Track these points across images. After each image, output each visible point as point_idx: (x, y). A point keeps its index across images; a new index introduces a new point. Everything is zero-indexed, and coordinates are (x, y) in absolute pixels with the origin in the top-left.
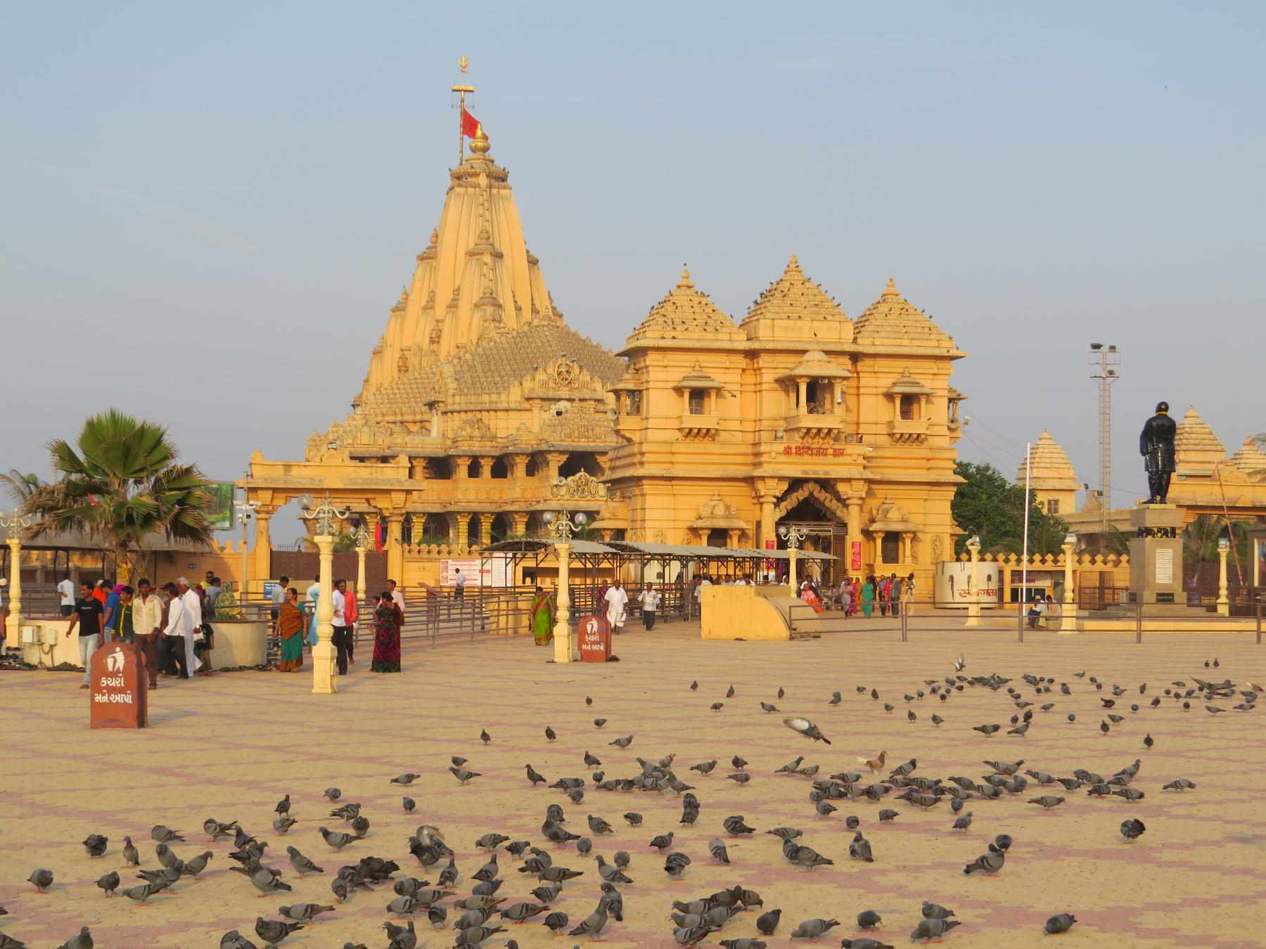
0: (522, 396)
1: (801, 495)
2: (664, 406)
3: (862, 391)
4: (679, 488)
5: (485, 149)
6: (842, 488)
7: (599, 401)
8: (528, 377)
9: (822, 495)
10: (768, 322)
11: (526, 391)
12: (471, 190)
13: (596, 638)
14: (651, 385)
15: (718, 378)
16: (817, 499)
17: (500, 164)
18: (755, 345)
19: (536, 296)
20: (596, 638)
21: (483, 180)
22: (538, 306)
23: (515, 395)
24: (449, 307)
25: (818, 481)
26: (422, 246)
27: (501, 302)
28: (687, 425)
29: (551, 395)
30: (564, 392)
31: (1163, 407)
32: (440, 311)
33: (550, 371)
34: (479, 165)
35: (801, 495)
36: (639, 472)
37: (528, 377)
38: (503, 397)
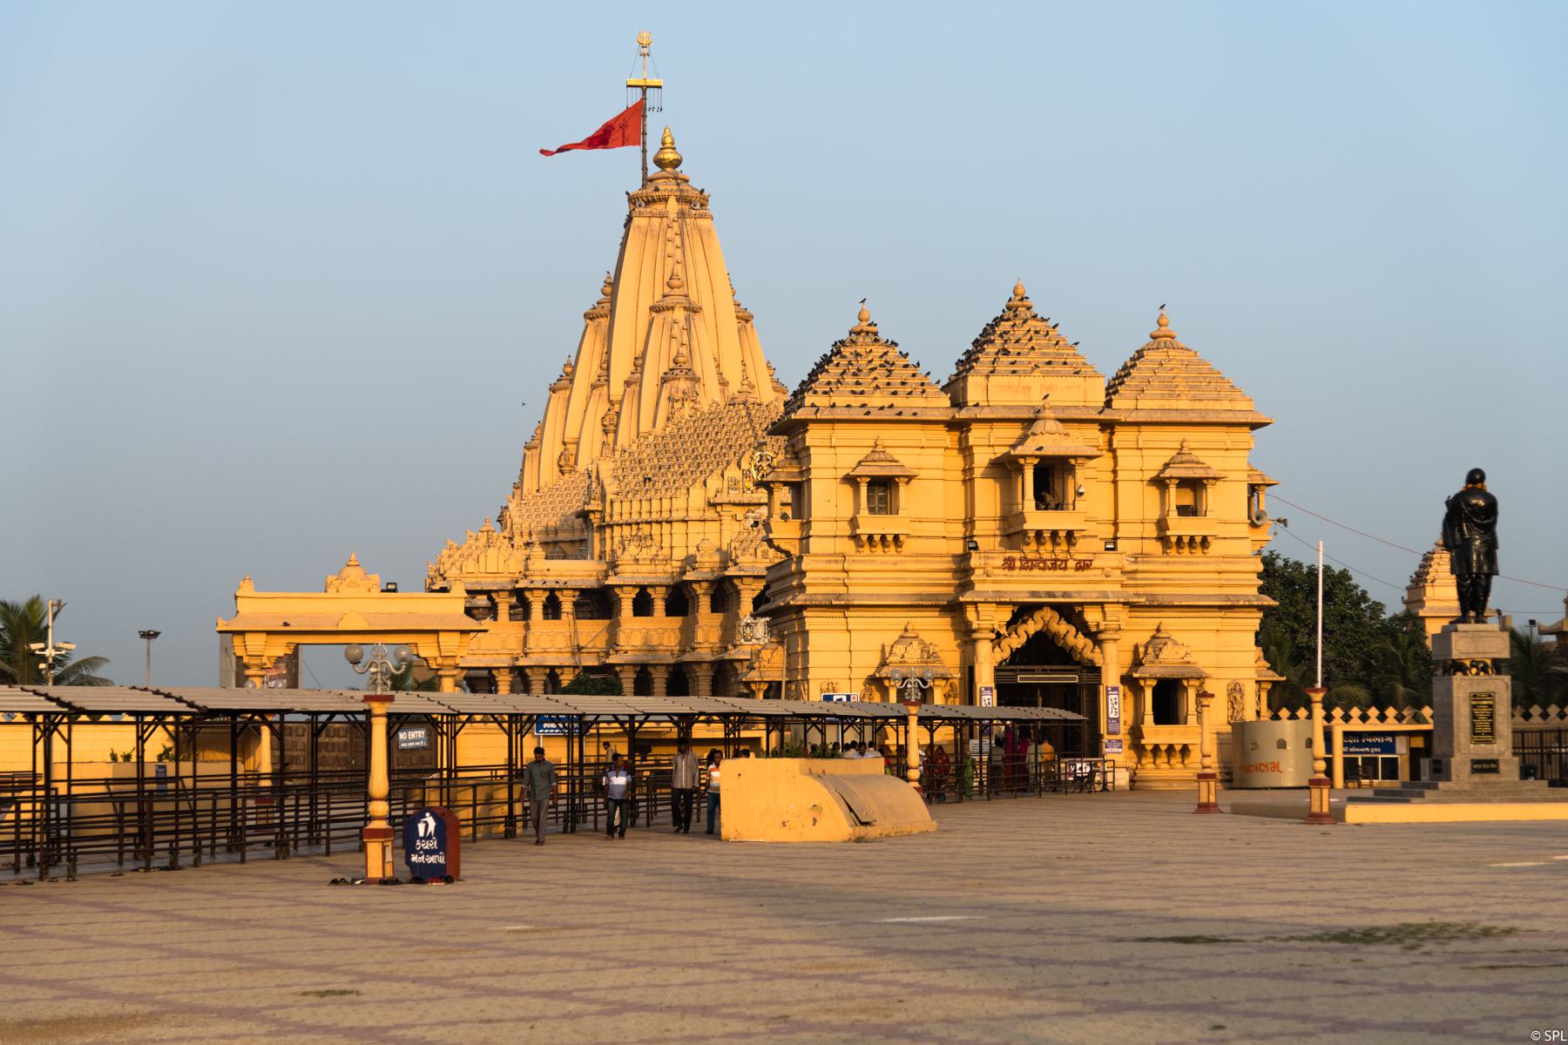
1: (1032, 627)
2: (830, 501)
3: (1121, 475)
4: (856, 620)
5: (676, 163)
6: (1092, 616)
9: (1062, 628)
10: (982, 379)
11: (711, 494)
12: (656, 221)
13: (433, 844)
14: (814, 474)
15: (908, 460)
16: (1055, 635)
17: (696, 183)
18: (963, 414)
19: (748, 361)
20: (433, 844)
21: (673, 206)
22: (752, 379)
23: (698, 497)
24: (628, 383)
25: (1055, 607)
26: (593, 296)
27: (699, 374)
28: (864, 530)
31: (1476, 477)
32: (617, 388)
33: (745, 465)
34: (666, 187)
35: (1032, 627)
36: (800, 600)
38: (679, 503)
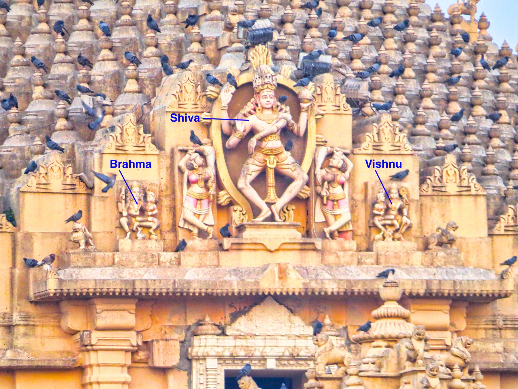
0: (18, 289)
7: (469, 303)
8: (54, 168)
29: (195, 272)
30: (272, 257)
37: (54, 168)
